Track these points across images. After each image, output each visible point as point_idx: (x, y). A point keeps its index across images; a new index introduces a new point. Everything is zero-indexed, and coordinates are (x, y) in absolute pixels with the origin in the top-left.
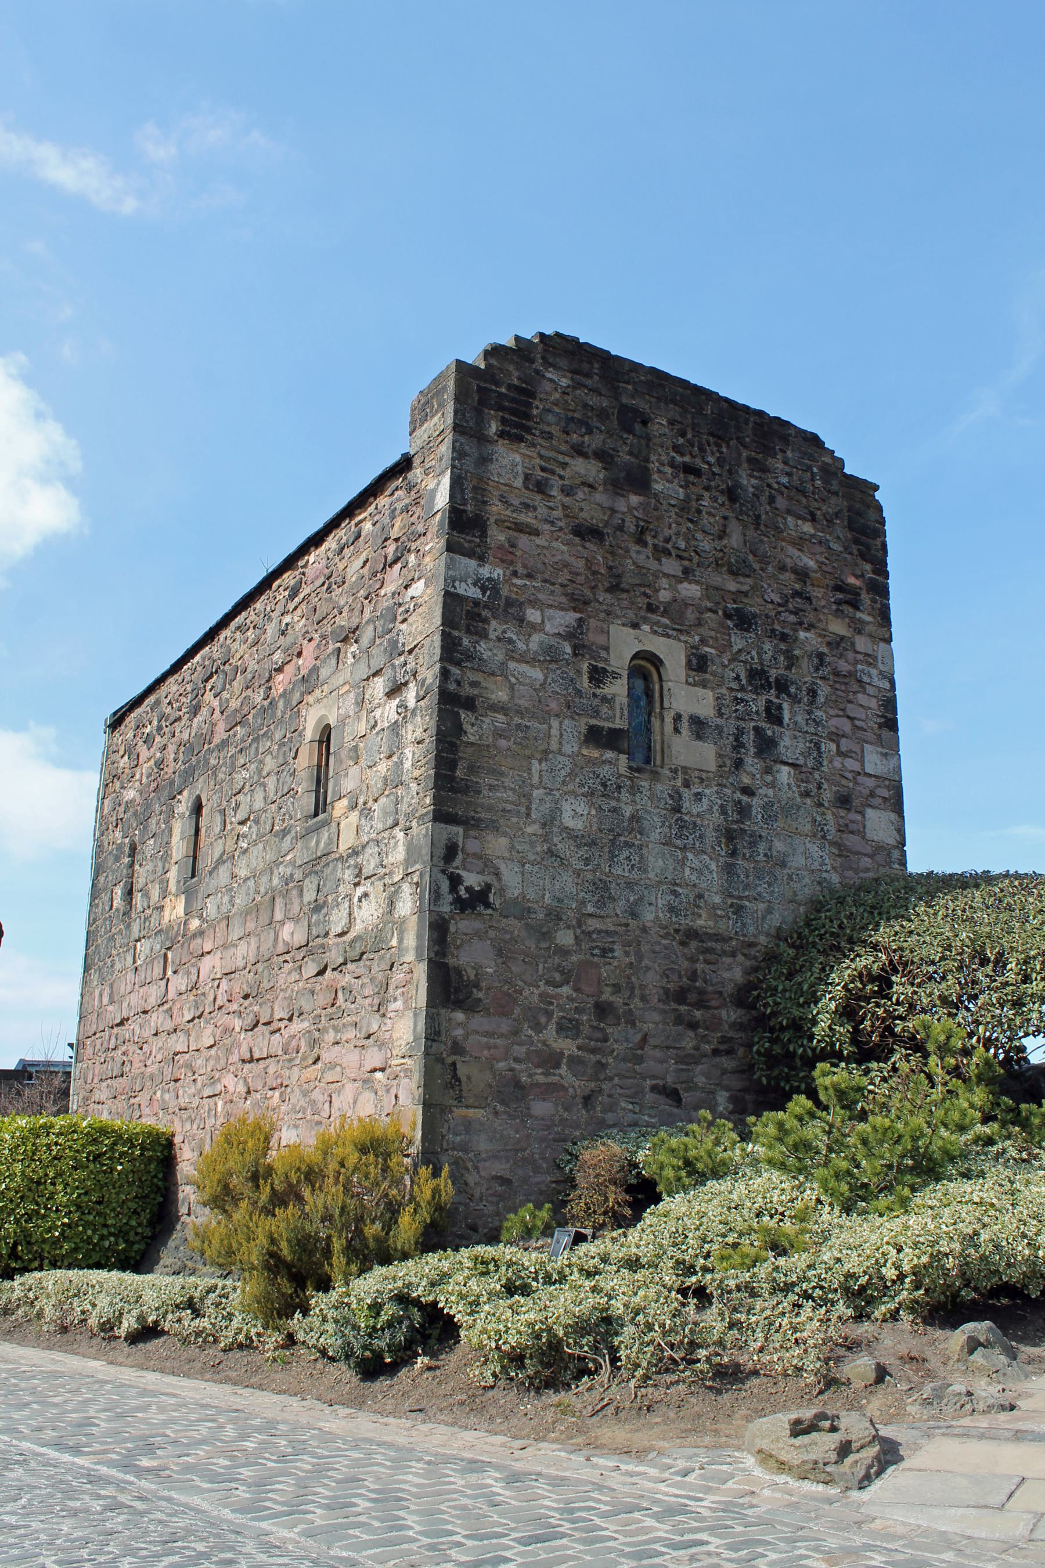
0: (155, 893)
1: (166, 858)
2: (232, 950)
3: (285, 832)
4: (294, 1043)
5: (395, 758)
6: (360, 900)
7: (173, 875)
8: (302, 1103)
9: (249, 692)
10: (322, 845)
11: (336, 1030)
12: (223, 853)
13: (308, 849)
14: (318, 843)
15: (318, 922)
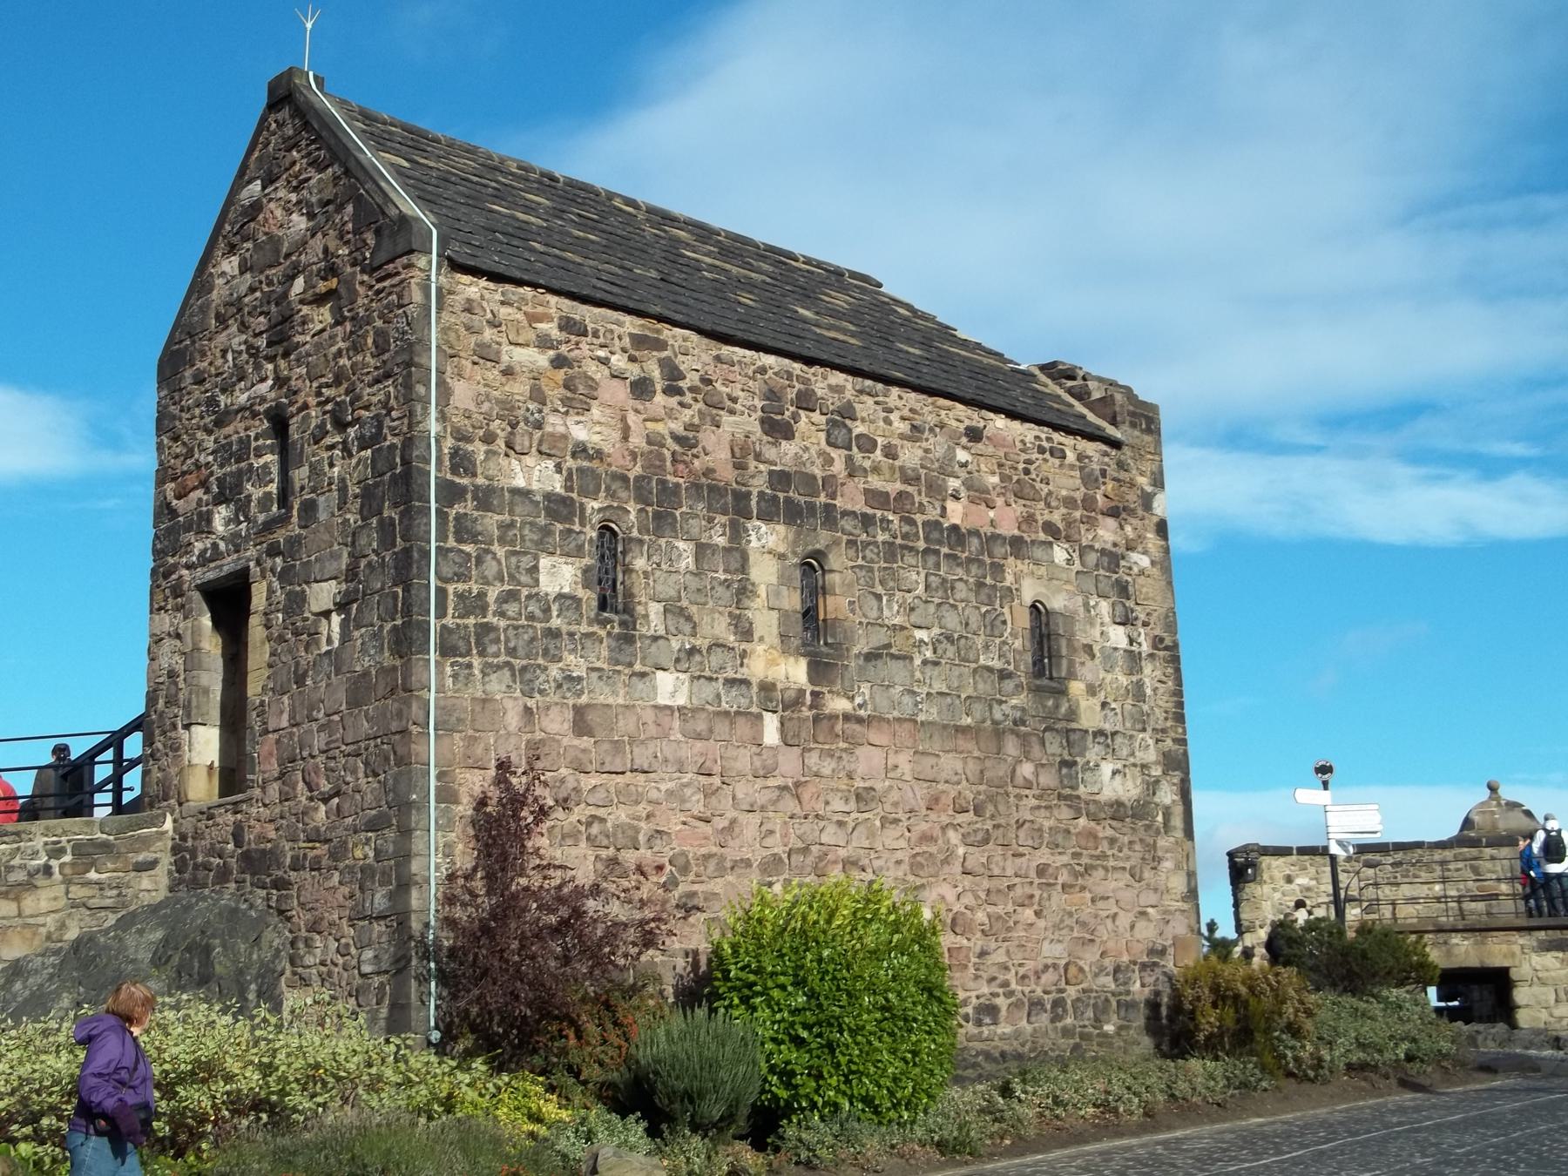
0: (718, 627)
1: (744, 591)
2: (933, 760)
3: (1004, 675)
4: (1051, 870)
5: (1134, 679)
6: (1114, 773)
7: (765, 622)
8: (1068, 922)
9: (910, 489)
10: (1063, 710)
11: (1106, 869)
12: (889, 646)
13: (1044, 707)
14: (1057, 707)
15: (1070, 776)
